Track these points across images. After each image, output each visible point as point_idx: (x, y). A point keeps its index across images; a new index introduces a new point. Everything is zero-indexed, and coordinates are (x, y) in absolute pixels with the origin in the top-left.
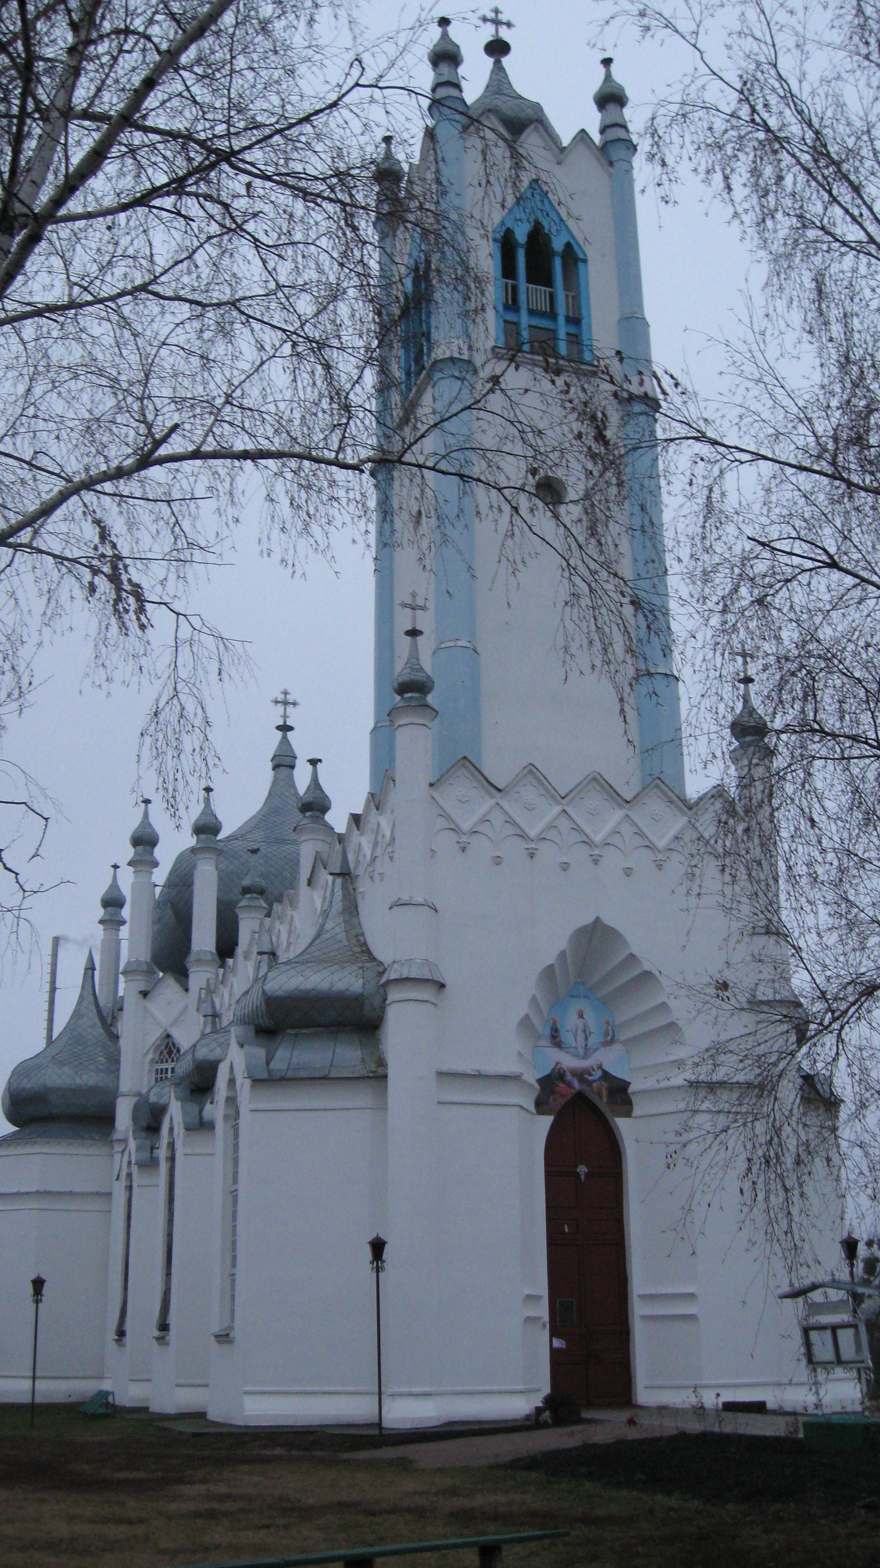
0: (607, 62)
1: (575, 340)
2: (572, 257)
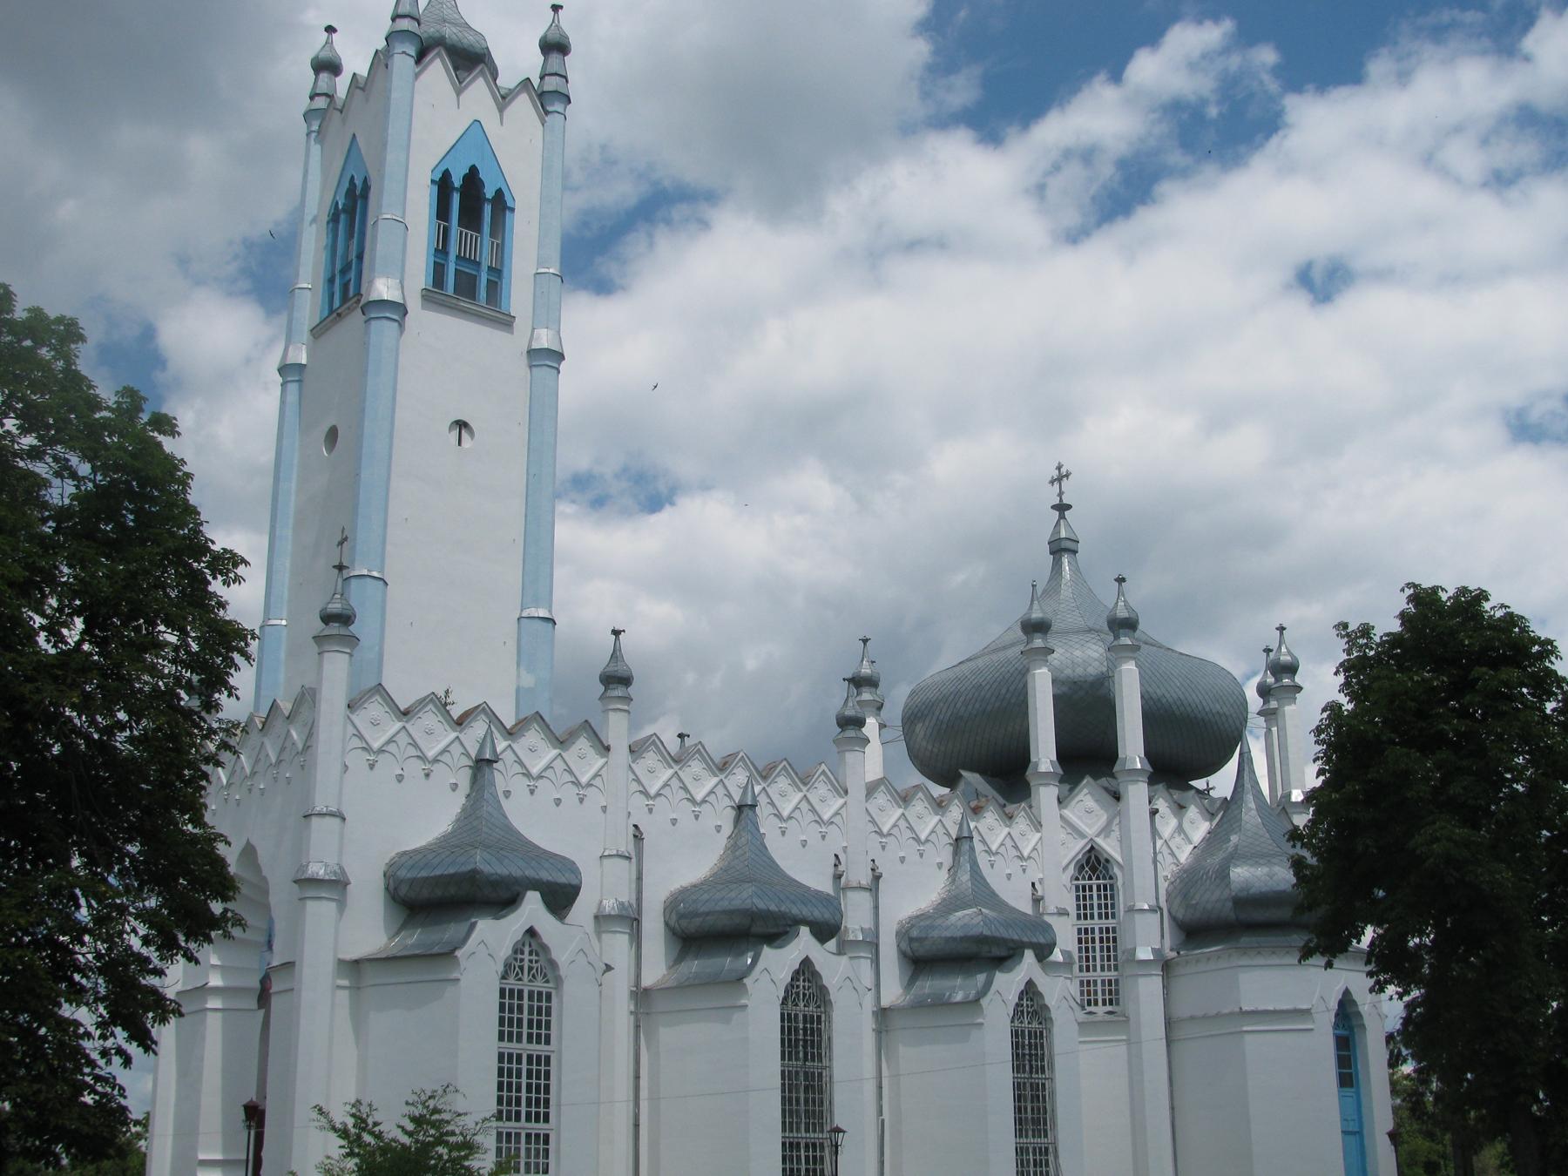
0: (556, 8)
1: (494, 288)
2: (501, 204)
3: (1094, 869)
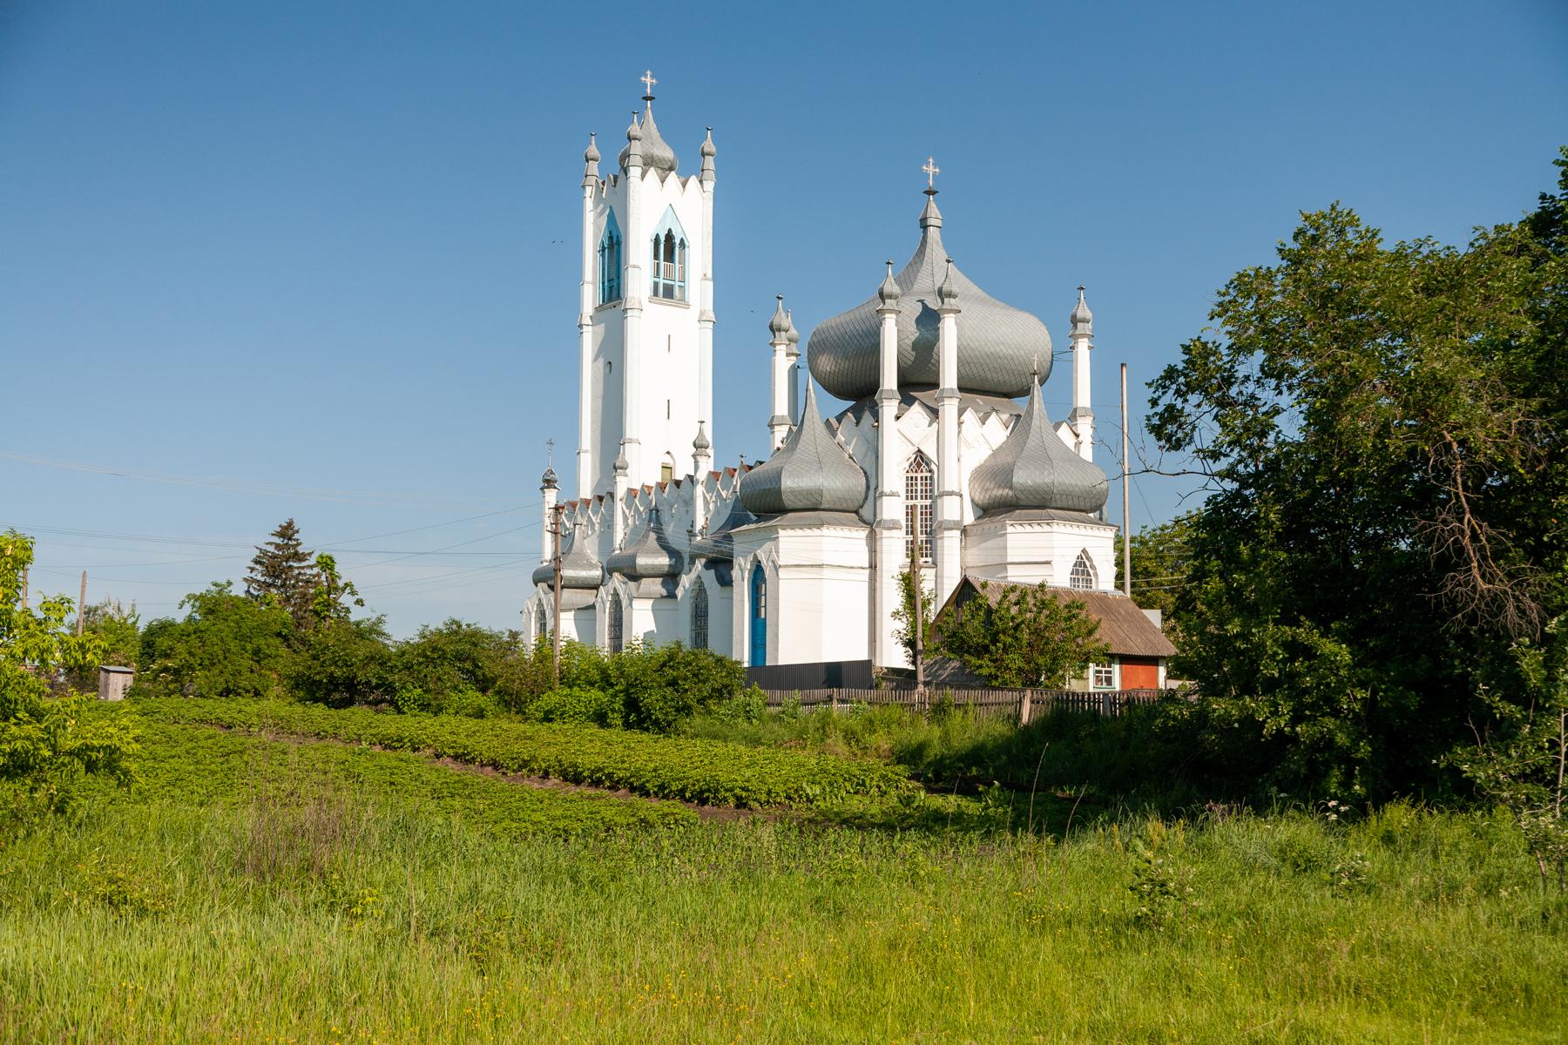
3: (919, 465)
